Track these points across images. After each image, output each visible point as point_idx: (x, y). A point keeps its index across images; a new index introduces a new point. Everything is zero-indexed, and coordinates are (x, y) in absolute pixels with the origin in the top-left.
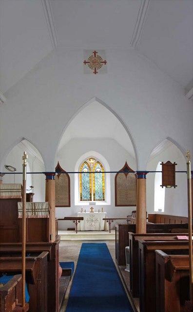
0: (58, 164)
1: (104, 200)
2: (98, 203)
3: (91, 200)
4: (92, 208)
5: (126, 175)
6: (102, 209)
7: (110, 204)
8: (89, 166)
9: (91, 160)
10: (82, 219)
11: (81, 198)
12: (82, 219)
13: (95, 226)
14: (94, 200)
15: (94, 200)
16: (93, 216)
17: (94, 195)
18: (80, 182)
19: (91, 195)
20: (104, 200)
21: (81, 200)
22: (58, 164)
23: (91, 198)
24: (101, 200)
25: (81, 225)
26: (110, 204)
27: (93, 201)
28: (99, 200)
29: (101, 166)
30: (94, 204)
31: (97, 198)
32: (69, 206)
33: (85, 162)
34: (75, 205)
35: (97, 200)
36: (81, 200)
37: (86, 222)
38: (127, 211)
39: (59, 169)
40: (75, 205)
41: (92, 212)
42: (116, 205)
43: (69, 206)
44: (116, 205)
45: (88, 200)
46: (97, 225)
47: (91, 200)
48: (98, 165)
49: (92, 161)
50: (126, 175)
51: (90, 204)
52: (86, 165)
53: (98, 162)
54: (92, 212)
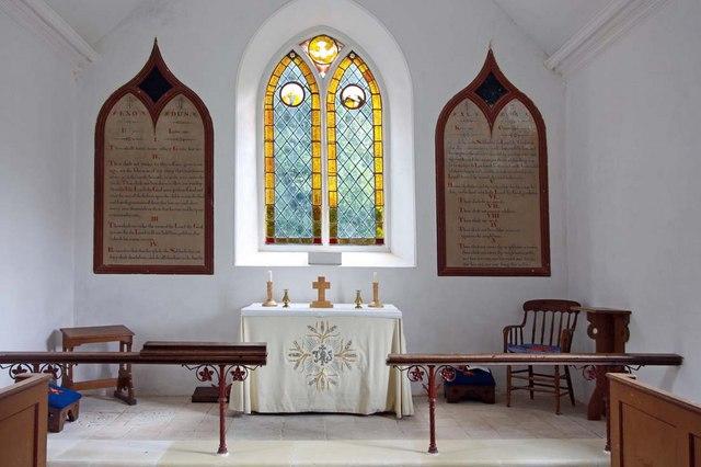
0: (156, 52)
1: (380, 242)
2: (353, 257)
3: (318, 241)
4: (321, 284)
5: (491, 118)
6: (374, 288)
7: (411, 264)
8: (309, 74)
9: (322, 44)
10: (257, 355)
11: (271, 226)
12: (257, 355)
13: (339, 388)
14: (333, 242)
15: (333, 242)
16: (327, 328)
17: (333, 216)
18: (267, 150)
19: (316, 214)
20: (380, 242)
21: (270, 241)
22: (156, 51)
23: (318, 231)
24: (367, 242)
25: (256, 387)
26: (411, 264)
27: (326, 246)
28: (358, 242)
29: (369, 76)
30: (335, 261)
31: (347, 231)
32: (207, 268)
33: (292, 55)
34: (240, 262)
35: (346, 242)
36: (270, 241)
37: (289, 363)
38: (501, 297)
39: (155, 84)
40: (240, 262)
41: (321, 302)
42: (443, 270)
43: (207, 268)
44: (443, 270)
45: (305, 241)
46: (351, 378)
47: (318, 241)
48: (355, 73)
49: (322, 51)
50: (491, 118)
51: (314, 261)
52: (294, 69)
53: (353, 57)
54: (321, 302)
